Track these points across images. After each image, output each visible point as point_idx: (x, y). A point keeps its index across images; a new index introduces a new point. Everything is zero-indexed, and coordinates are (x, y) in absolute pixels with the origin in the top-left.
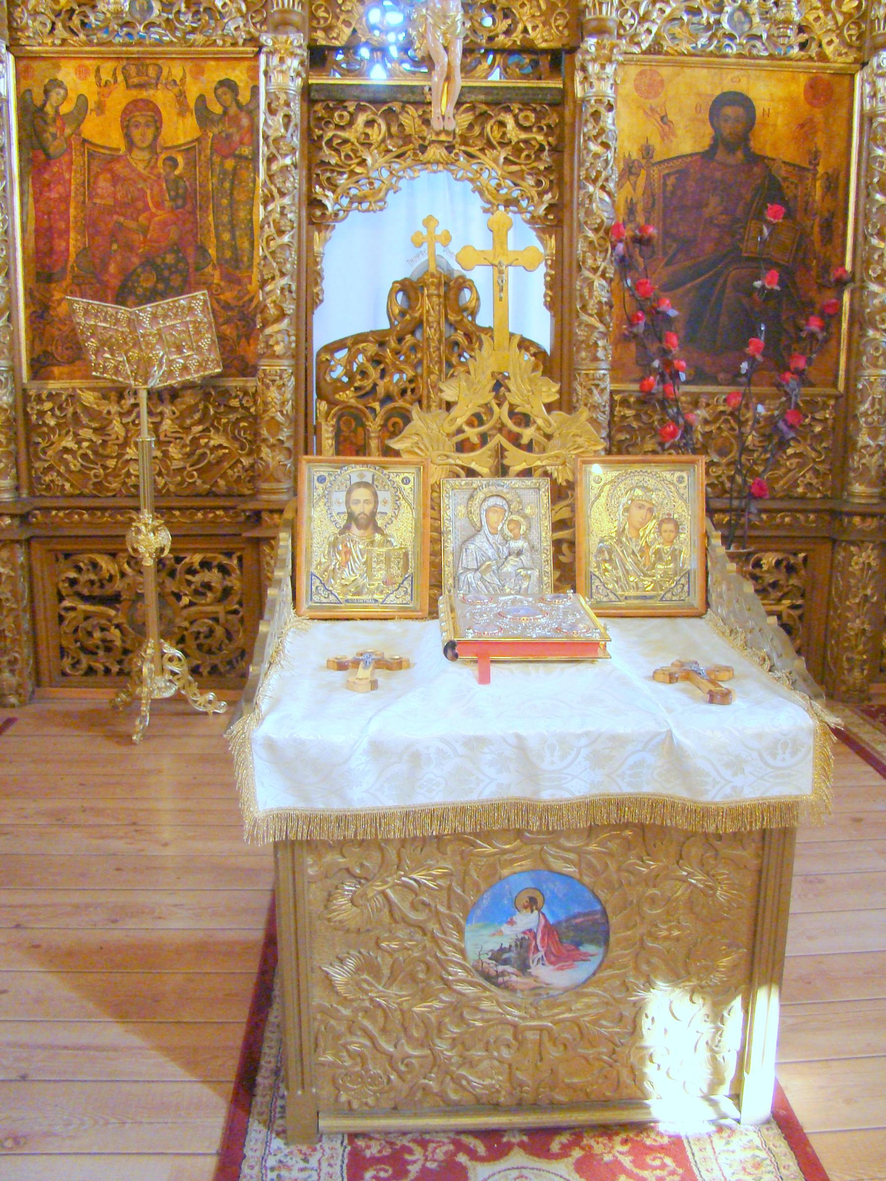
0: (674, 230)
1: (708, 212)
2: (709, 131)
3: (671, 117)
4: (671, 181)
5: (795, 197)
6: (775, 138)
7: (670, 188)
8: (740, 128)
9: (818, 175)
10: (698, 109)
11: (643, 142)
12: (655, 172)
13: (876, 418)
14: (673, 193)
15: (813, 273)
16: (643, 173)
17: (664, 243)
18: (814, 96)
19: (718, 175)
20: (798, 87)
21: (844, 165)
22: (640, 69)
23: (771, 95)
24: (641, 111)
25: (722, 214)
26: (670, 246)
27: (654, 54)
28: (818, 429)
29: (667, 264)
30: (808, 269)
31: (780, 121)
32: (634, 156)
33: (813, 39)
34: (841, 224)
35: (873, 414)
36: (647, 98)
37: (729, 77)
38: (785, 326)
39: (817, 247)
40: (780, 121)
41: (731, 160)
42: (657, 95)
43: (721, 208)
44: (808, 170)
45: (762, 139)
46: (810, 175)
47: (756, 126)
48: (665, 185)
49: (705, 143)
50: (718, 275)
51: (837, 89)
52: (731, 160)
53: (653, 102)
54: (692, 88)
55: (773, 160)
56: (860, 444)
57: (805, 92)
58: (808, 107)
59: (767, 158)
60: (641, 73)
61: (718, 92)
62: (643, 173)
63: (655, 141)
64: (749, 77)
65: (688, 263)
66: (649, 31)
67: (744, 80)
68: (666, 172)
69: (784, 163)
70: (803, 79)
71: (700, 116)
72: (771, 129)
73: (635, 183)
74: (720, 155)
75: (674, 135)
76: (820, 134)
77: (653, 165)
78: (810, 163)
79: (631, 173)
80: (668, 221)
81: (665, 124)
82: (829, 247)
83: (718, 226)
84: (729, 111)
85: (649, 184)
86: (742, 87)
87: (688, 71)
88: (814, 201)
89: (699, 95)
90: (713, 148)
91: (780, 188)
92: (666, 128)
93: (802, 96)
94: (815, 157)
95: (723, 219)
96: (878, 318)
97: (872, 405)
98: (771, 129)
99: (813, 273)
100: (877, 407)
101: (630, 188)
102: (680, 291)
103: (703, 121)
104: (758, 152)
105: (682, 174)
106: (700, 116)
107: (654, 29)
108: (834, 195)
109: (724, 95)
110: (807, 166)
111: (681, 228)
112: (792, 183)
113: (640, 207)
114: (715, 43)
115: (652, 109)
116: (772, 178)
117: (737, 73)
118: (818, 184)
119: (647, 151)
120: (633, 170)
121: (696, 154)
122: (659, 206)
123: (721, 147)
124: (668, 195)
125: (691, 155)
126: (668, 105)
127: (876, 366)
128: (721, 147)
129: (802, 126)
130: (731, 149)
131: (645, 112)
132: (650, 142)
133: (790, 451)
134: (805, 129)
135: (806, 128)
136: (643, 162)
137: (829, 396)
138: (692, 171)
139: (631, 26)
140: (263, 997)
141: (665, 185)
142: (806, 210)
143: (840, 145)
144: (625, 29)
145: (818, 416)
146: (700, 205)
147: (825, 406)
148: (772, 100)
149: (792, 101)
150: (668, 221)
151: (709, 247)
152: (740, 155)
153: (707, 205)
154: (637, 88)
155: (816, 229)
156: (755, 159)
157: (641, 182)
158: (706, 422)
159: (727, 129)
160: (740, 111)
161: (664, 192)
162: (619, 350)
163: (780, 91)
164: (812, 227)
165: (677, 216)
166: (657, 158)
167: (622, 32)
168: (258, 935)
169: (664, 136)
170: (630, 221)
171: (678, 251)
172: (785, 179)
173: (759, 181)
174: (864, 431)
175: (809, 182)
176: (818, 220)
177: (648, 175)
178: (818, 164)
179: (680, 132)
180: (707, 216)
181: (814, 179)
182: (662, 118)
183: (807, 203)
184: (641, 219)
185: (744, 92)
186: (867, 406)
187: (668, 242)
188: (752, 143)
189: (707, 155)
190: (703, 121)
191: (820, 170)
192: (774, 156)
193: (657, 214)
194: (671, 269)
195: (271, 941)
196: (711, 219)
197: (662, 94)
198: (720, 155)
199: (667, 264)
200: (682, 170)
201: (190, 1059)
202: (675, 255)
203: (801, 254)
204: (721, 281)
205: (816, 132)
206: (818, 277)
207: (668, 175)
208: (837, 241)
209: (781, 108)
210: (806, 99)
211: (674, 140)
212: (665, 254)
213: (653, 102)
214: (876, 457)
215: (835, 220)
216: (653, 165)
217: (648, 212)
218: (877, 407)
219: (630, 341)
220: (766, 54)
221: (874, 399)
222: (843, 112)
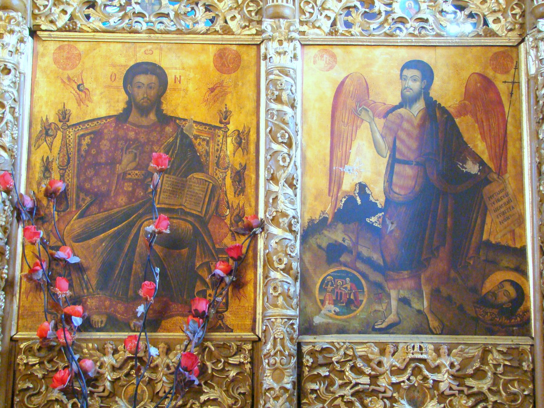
0: (87, 186)
1: (119, 169)
2: (123, 97)
3: (87, 85)
4: (87, 140)
5: (208, 153)
6: (187, 101)
7: (84, 147)
8: (153, 93)
9: (229, 133)
10: (113, 77)
11: (60, 107)
12: (72, 134)
13: (278, 360)
14: (88, 152)
15: (228, 221)
16: (60, 134)
17: (78, 197)
18: (223, 65)
19: (132, 135)
20: (208, 58)
21: (254, 122)
22: (58, 45)
23: (182, 64)
24: (59, 81)
25: (135, 169)
26: (84, 200)
27: (69, 31)
28: (233, 373)
29: (81, 216)
30: (221, 217)
31: (191, 87)
32: (51, 120)
33: (218, 15)
34: (253, 176)
35: (275, 354)
36: (64, 69)
37: (143, 50)
38: (200, 273)
39: (230, 196)
40: (191, 87)
41: (144, 121)
42: (74, 66)
43: (134, 165)
44: (220, 128)
45: (173, 103)
46: (221, 133)
47: (168, 91)
48: (80, 144)
49: (120, 107)
50: (130, 226)
51: (245, 57)
52: (144, 121)
53: (70, 72)
54: (107, 60)
55: (185, 120)
56: (265, 386)
57: (215, 61)
58: (218, 73)
59: (180, 119)
60: (60, 48)
61: (132, 63)
62: (60, 134)
63: (72, 106)
64: (161, 49)
65: (101, 215)
66: (64, 12)
67: (157, 52)
68: (82, 133)
69: (195, 122)
70: (212, 50)
71: (115, 84)
72: (182, 93)
73: (52, 143)
74: (134, 117)
75: (90, 100)
76: (229, 96)
77: (69, 127)
78: (221, 122)
79: (47, 134)
80: (82, 178)
81: (82, 91)
82: (242, 197)
83: (130, 180)
84: (143, 79)
85: (65, 144)
86: (155, 58)
87: (104, 46)
88: (226, 155)
89: (114, 65)
90: (127, 112)
91: (191, 146)
92: (83, 95)
93: (212, 64)
94: (225, 117)
95: (137, 174)
96: (275, 258)
97: (275, 346)
98: (182, 93)
99: (228, 221)
100: (279, 347)
101: (47, 148)
102: (92, 242)
103: (117, 88)
104: (170, 114)
105: (97, 135)
106: (115, 84)
107: (70, 10)
108: (246, 150)
109: (138, 65)
110: (218, 124)
111: (94, 183)
112: (204, 140)
113: (55, 165)
114: (127, 21)
115: (69, 79)
116: (184, 136)
117: (150, 47)
118: (229, 140)
119: (64, 116)
120: (50, 132)
121: (110, 117)
122: (75, 162)
123: (134, 110)
124: (83, 153)
125: (105, 118)
126: (84, 75)
127: (276, 306)
128: (134, 110)
129: (212, 90)
130: (144, 111)
131: (63, 82)
132: (67, 107)
133: (203, 398)
134: (216, 92)
135: (216, 91)
136: (60, 124)
137: (246, 341)
138: (106, 131)
139: (45, 6)
141: (80, 144)
142: (217, 164)
143: (250, 105)
144: (39, 10)
145: (231, 361)
146: (113, 162)
147: (239, 350)
148: (183, 69)
149: (202, 69)
150: (82, 178)
151: (122, 200)
152: (152, 117)
153: (120, 163)
154: (56, 61)
155: (228, 181)
156: (166, 120)
157: (57, 143)
158: (114, 369)
159: (140, 95)
160: (154, 78)
161: (79, 150)
162: (30, 298)
163: (190, 61)
164: (224, 179)
165: (90, 173)
166: (73, 121)
167: (36, 11)
169: (80, 102)
170: (45, 177)
171: (91, 204)
172: (196, 137)
173: (171, 140)
174: (268, 373)
175: (220, 139)
176: (229, 173)
177: (64, 137)
178: (229, 123)
179: (95, 98)
180: (120, 172)
181: (226, 136)
182: (78, 86)
183: (219, 157)
184: (56, 175)
185: (157, 63)
186: (269, 346)
187: (82, 195)
188: (164, 107)
189: (121, 118)
190: (117, 88)
191: (231, 127)
192: (186, 118)
193: (71, 172)
194: (84, 221)
196: (125, 174)
197: (79, 66)
198: (134, 117)
199: (81, 216)
200: (96, 131)
202: (88, 207)
203: (214, 204)
204: (134, 231)
205: (226, 94)
206: (231, 224)
207: (83, 136)
208: (250, 190)
209: (192, 75)
210: (215, 66)
211: (90, 104)
212: (78, 207)
213: (70, 72)
214: (281, 401)
215: (246, 172)
216: (69, 127)
217: (63, 168)
218: (279, 347)
219: (41, 290)
220: (173, 28)
221: (275, 339)
222: (251, 77)
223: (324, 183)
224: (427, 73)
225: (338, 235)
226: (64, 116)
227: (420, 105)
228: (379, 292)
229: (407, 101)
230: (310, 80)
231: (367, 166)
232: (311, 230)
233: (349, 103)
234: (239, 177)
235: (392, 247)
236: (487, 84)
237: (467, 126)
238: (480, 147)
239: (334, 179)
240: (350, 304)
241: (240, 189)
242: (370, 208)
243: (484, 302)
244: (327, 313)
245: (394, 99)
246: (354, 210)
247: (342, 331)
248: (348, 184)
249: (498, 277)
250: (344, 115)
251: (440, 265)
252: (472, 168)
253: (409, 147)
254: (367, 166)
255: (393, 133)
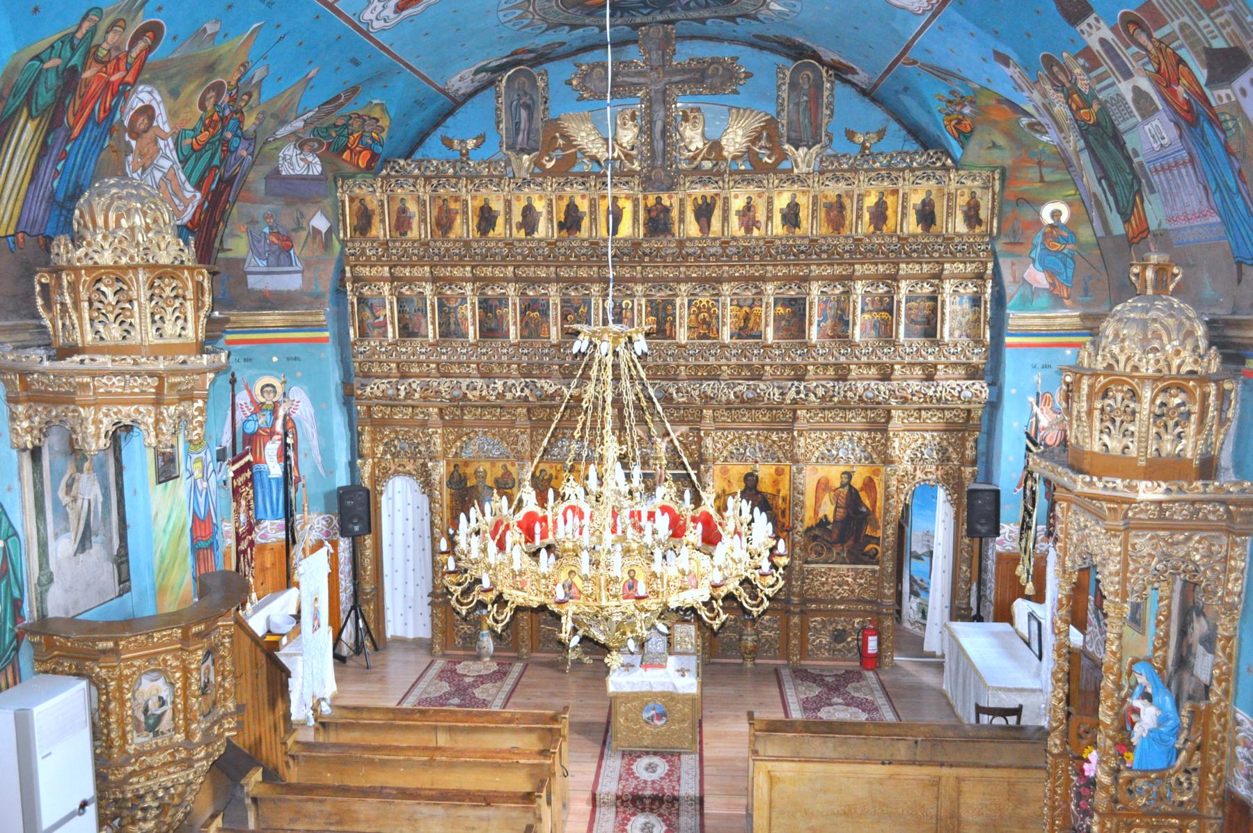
94: (779, 491)
130: (751, 489)
134: (776, 483)
140: (607, 731)
168: (604, 720)
195: (608, 722)
201: (594, 741)
223: (812, 514)
224: (849, 475)
225: (817, 532)
226: (724, 491)
227: (846, 489)
228: (830, 550)
229: (842, 486)
230: (809, 480)
231: (828, 509)
232: (809, 529)
233: (823, 486)
234: (783, 512)
235: (835, 536)
236: (871, 480)
237: (863, 495)
238: (867, 502)
239: (816, 513)
240: (820, 554)
241: (784, 516)
242: (828, 523)
243: (864, 554)
244: (813, 557)
245: (838, 485)
246: (823, 523)
247: (817, 563)
248: (821, 515)
249: (870, 546)
250: (820, 491)
251: (850, 542)
252: (864, 510)
253: (842, 502)
254: (828, 509)
255: (837, 496)
